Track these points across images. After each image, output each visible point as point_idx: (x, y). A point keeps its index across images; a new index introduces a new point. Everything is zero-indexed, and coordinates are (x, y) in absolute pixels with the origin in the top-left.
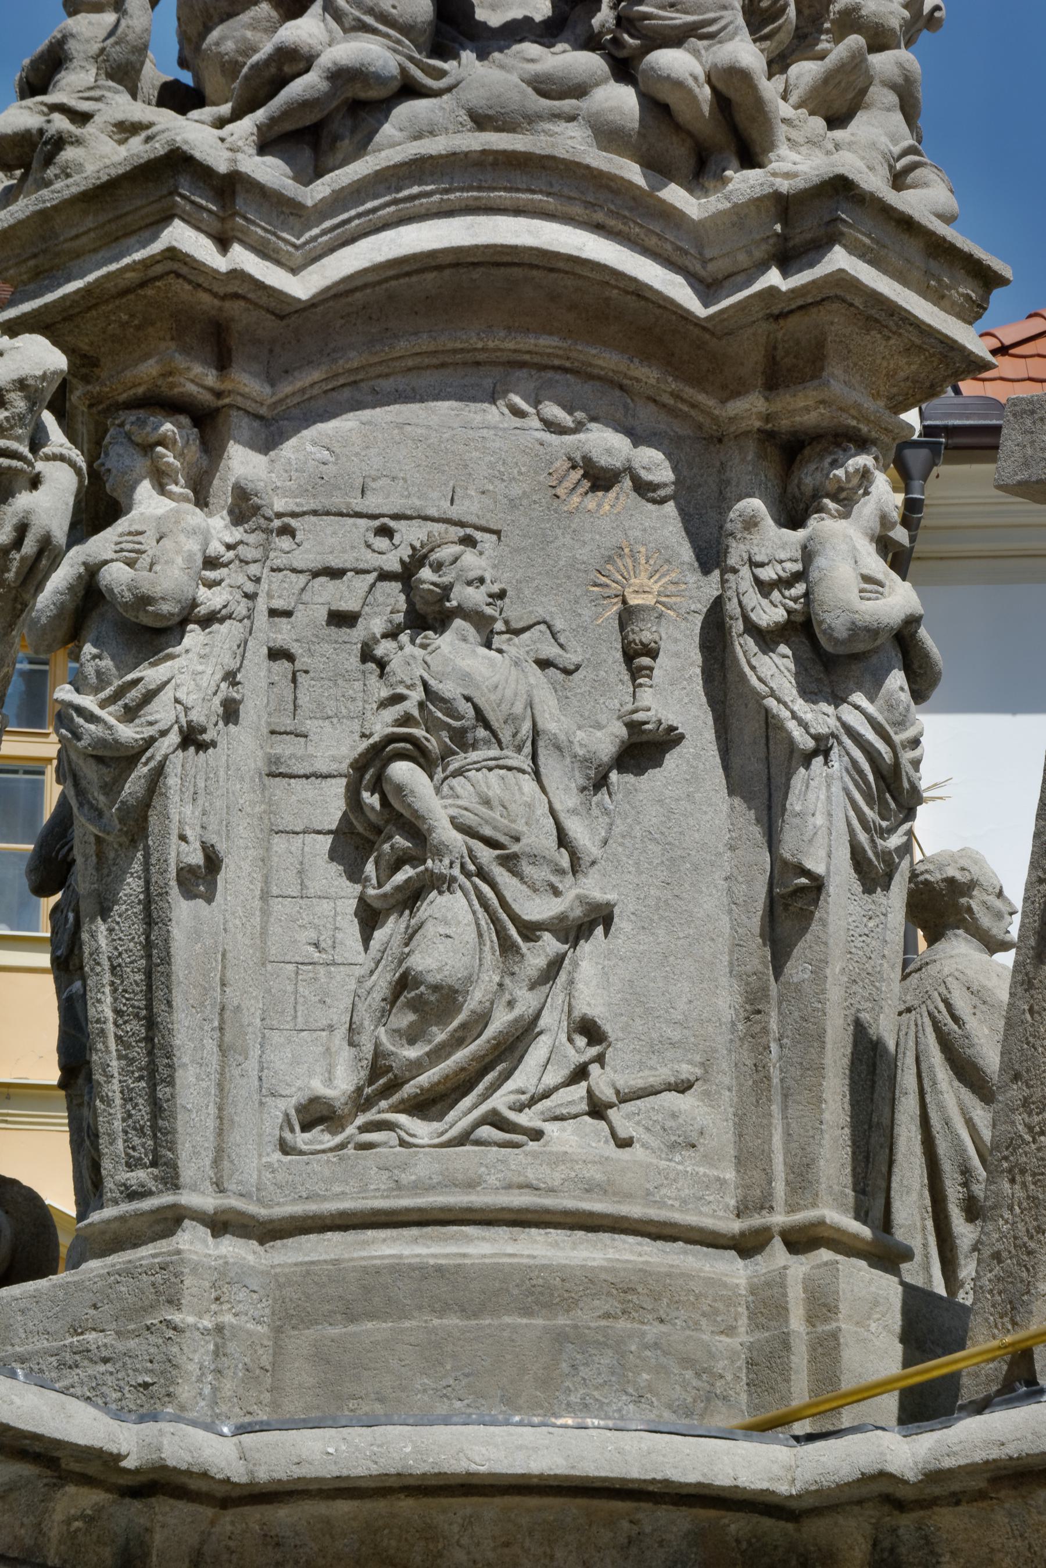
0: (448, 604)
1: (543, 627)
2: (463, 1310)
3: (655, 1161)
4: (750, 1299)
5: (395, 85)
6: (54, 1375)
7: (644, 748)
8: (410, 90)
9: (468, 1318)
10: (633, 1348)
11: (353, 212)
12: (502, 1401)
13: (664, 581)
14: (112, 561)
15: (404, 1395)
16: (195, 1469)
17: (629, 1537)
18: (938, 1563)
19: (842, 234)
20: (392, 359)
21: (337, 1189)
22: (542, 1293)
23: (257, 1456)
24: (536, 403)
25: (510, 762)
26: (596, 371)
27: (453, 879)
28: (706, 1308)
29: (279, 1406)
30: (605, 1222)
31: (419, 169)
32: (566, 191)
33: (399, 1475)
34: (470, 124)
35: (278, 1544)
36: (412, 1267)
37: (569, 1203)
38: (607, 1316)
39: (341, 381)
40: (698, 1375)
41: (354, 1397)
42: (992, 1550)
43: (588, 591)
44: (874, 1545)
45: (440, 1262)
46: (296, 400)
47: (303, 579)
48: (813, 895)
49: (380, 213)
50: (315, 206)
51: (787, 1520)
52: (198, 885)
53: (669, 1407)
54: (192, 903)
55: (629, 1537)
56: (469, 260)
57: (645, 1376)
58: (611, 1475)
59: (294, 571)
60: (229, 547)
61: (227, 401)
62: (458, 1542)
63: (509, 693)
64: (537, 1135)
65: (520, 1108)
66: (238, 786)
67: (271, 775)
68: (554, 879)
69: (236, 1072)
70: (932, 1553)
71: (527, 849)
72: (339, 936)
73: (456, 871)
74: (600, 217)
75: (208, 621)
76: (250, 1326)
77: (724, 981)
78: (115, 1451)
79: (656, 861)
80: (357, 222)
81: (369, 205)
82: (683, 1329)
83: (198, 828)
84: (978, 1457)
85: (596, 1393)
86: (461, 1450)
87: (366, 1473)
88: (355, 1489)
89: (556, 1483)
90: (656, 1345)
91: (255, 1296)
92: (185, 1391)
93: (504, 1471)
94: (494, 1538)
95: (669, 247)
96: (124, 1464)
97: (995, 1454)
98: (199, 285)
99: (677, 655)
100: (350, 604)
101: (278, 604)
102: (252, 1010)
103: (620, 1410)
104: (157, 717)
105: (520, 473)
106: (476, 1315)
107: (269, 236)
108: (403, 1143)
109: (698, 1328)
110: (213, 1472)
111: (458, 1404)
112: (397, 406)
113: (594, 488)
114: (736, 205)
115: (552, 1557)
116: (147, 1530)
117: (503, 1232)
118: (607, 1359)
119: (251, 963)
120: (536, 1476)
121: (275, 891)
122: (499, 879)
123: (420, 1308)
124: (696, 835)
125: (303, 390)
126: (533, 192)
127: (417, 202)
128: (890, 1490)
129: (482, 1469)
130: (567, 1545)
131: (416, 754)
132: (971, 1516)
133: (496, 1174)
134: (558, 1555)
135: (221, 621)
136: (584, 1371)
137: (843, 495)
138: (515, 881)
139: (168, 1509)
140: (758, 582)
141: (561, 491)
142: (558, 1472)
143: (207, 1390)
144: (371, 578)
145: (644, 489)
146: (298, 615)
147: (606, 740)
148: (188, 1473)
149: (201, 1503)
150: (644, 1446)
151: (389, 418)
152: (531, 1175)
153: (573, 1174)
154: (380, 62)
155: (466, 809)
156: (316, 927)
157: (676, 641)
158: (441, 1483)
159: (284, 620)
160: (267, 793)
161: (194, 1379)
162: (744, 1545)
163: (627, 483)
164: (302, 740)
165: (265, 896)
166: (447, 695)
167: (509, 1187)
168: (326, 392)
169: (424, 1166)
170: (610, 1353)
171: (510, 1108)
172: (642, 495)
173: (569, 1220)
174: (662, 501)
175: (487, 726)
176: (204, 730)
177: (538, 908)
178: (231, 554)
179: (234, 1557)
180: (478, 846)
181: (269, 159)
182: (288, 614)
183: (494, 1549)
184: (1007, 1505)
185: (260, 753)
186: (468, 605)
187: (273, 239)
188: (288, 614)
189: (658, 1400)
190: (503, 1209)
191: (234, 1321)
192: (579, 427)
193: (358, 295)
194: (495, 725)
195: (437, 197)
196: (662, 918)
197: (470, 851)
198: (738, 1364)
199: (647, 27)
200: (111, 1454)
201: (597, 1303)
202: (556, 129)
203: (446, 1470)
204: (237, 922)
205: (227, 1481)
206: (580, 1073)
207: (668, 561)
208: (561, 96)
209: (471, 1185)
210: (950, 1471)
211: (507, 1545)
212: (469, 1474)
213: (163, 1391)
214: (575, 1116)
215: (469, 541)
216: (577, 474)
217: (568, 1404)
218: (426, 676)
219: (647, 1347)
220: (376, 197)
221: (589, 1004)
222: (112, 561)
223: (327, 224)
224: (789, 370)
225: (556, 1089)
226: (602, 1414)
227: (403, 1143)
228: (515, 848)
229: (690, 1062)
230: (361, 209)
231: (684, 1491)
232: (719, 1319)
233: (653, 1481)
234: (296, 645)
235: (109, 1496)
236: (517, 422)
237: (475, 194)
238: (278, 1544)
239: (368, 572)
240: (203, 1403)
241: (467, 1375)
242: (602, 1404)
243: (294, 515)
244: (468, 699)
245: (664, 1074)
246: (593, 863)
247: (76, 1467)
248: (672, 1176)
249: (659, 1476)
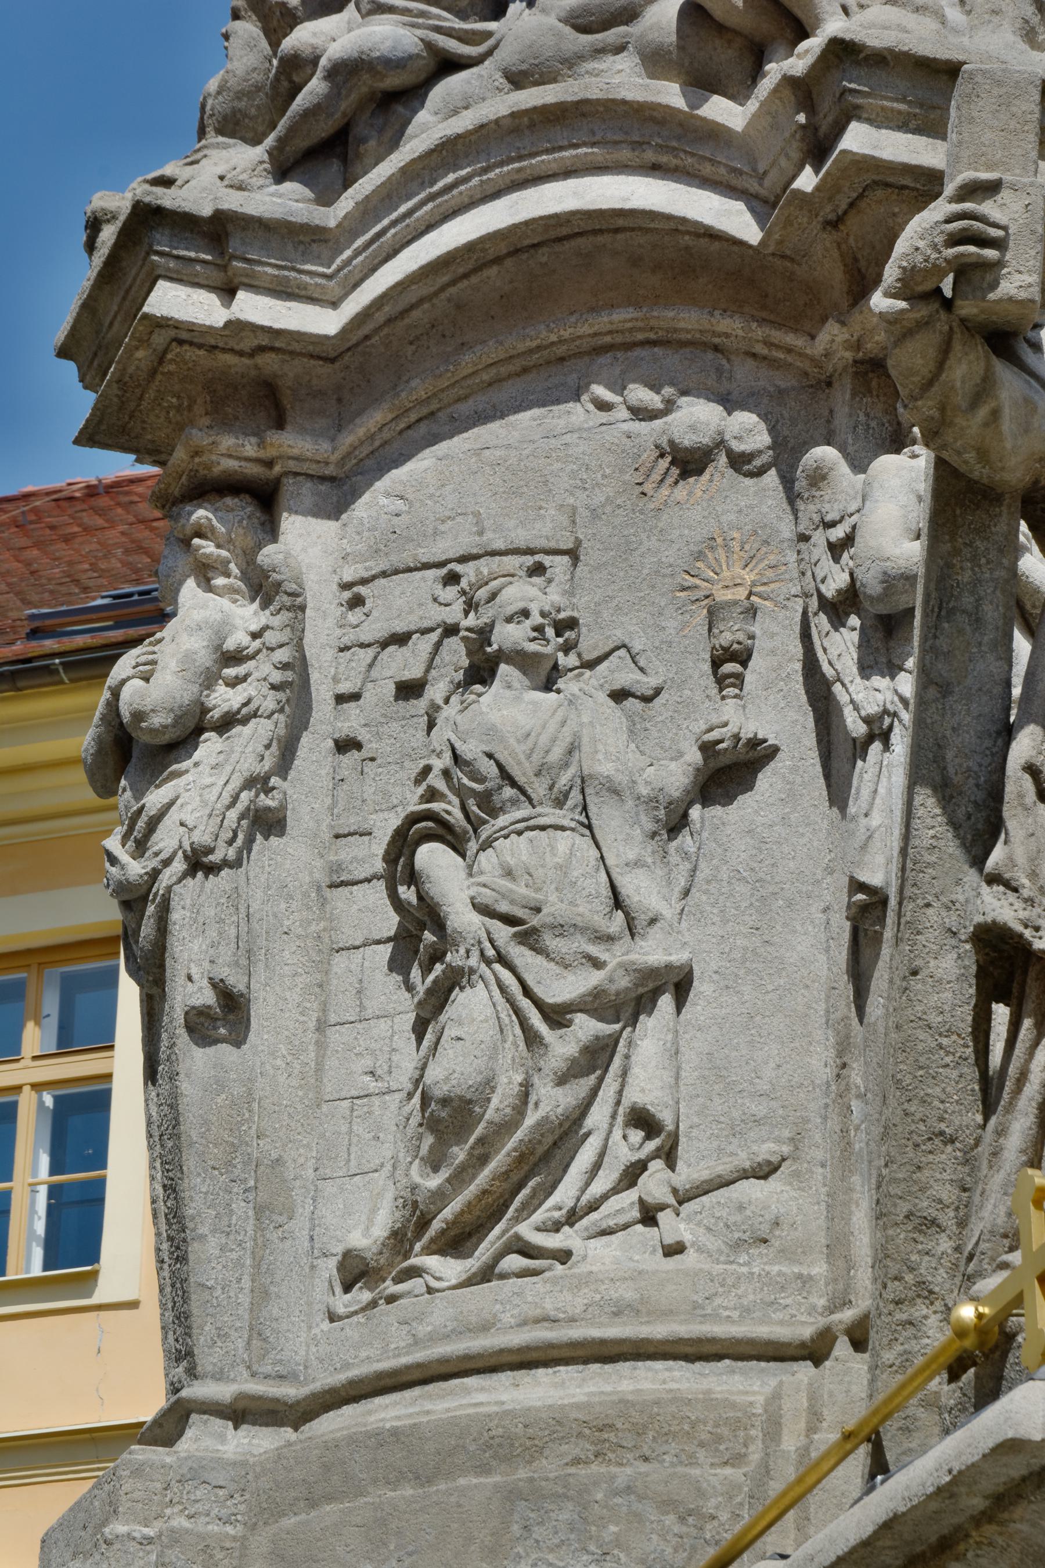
0: (489, 649)
1: (622, 652)
2: (417, 1478)
3: (706, 1267)
5: (427, 64)
7: (729, 772)
8: (448, 65)
9: (422, 1486)
10: (599, 1496)
11: (386, 222)
13: (761, 566)
14: (129, 679)
19: (857, 107)
20: (465, 378)
22: (500, 1445)
24: (620, 390)
25: (541, 821)
26: (683, 336)
27: (472, 971)
28: (704, 1436)
30: (625, 1349)
31: (449, 152)
32: (610, 136)
34: (508, 86)
36: (369, 1435)
37: (576, 1333)
38: (577, 1461)
39: (413, 417)
40: (682, 1519)
43: (675, 598)
45: (395, 1424)
46: (365, 450)
47: (371, 652)
48: (878, 912)
50: (339, 225)
52: (215, 1028)
54: (211, 1050)
56: (527, 242)
57: (613, 1528)
59: (363, 646)
60: (255, 636)
61: (277, 469)
63: (544, 740)
64: (564, 1256)
65: (556, 1227)
66: (283, 906)
67: (333, 886)
68: (594, 950)
69: (274, 1236)
71: (549, 920)
72: (395, 1058)
73: (474, 961)
74: (650, 156)
75: (227, 723)
76: (215, 1528)
77: (819, 1034)
79: (744, 904)
80: (393, 231)
81: (403, 209)
82: (673, 1465)
83: (206, 965)
85: (551, 1557)
90: (629, 1490)
91: (221, 1492)
95: (722, 170)
98: (215, 347)
99: (773, 652)
100: (415, 672)
101: (345, 688)
102: (302, 1160)
104: (161, 845)
105: (604, 476)
106: (429, 1481)
107: (286, 273)
109: (692, 1461)
112: (476, 430)
113: (685, 475)
117: (505, 1378)
118: (566, 1514)
119: (299, 1107)
121: (333, 1018)
122: (518, 962)
123: (375, 1481)
124: (792, 864)
125: (372, 437)
126: (576, 146)
127: (455, 192)
131: (441, 831)
133: (513, 1309)
135: (245, 721)
136: (538, 1532)
138: (540, 960)
141: (648, 487)
144: (434, 636)
145: (739, 462)
146: (366, 695)
147: (676, 775)
151: (467, 446)
152: (549, 1306)
153: (598, 1297)
154: (388, 44)
155: (485, 886)
156: (373, 1053)
157: (773, 635)
159: (353, 704)
160: (328, 908)
163: (723, 459)
164: (366, 838)
165: (322, 1026)
167: (524, 1323)
168: (401, 432)
169: (441, 1313)
170: (570, 1505)
171: (538, 1229)
172: (738, 470)
173: (580, 1353)
174: (760, 473)
175: (514, 784)
176: (210, 851)
177: (563, 987)
178: (257, 644)
180: (496, 925)
181: (289, 186)
182: (355, 697)
185: (319, 863)
186: (507, 645)
187: (293, 274)
188: (355, 697)
189: (628, 1555)
190: (502, 1351)
191: (186, 1524)
192: (670, 406)
193: (416, 314)
194: (521, 780)
195: (476, 181)
196: (749, 971)
198: (739, 1499)
201: (565, 1447)
204: (279, 1062)
206: (633, 1173)
207: (766, 542)
208: (605, 25)
209: (485, 1327)
214: (626, 1227)
215: (538, 570)
216: (664, 463)
218: (454, 739)
219: (617, 1493)
220: (409, 198)
221: (643, 1090)
222: (129, 679)
223: (359, 242)
225: (605, 1197)
227: (430, 1290)
228: (535, 921)
229: (778, 1140)
232: (722, 1447)
234: (363, 731)
236: (604, 417)
237: (516, 165)
239: (431, 630)
241: (410, 1554)
243: (364, 582)
244: (490, 756)
245: (743, 1160)
246: (653, 921)
248: (730, 1281)
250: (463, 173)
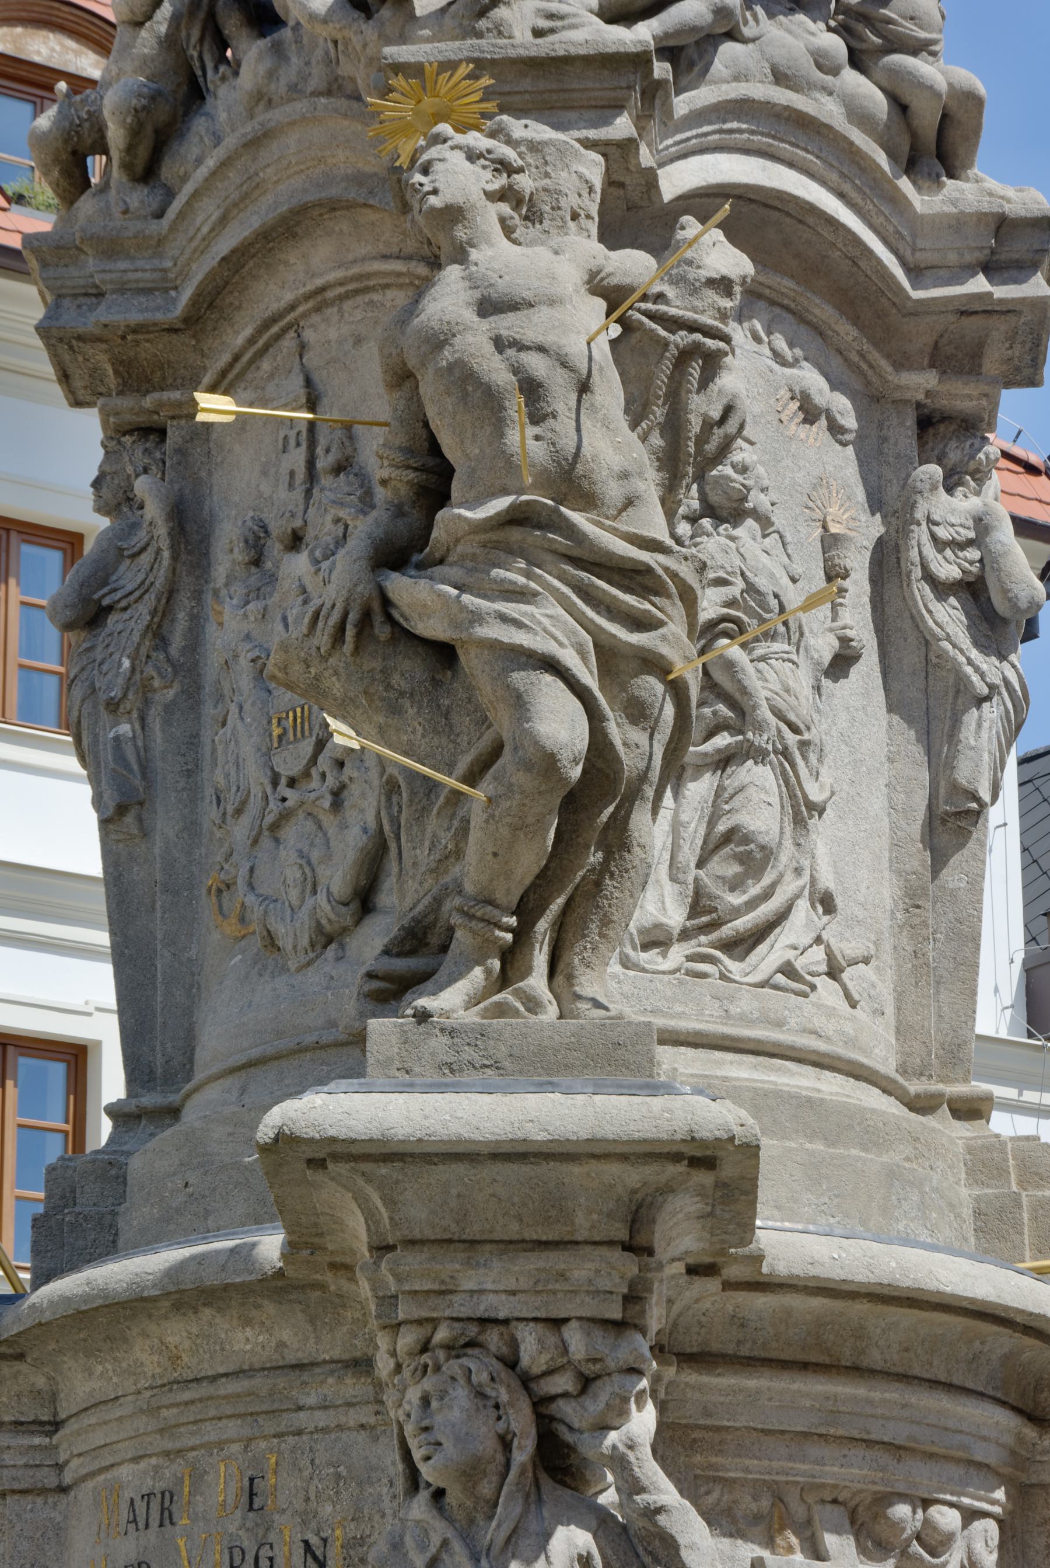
4: (968, 1157)
9: (829, 1146)
11: (694, 132)
21: (678, 1008)
24: (769, 333)
26: (810, 317)
32: (831, 159)
34: (771, 78)
35: (742, 1325)
36: (792, 1096)
48: (974, 818)
49: (710, 138)
74: (847, 188)
77: (886, 874)
87: (866, 1280)
88: (832, 1290)
95: (891, 229)
108: (723, 977)
113: (805, 421)
114: (962, 213)
123: (797, 1132)
129: (948, 1290)
134: (935, 1363)
137: (978, 476)
140: (934, 537)
141: (784, 418)
145: (835, 429)
158: (895, 1293)
166: (762, 589)
169: (746, 1002)
172: (833, 435)
174: (844, 444)
180: (784, 728)
192: (795, 364)
195: (745, 136)
197: (779, 731)
199: (891, 30)
202: (823, 100)
211: (906, 1350)
220: (710, 123)
224: (947, 357)
230: (700, 131)
238: (742, 1325)
241: (836, 1196)
244: (776, 596)
250: (744, 126)
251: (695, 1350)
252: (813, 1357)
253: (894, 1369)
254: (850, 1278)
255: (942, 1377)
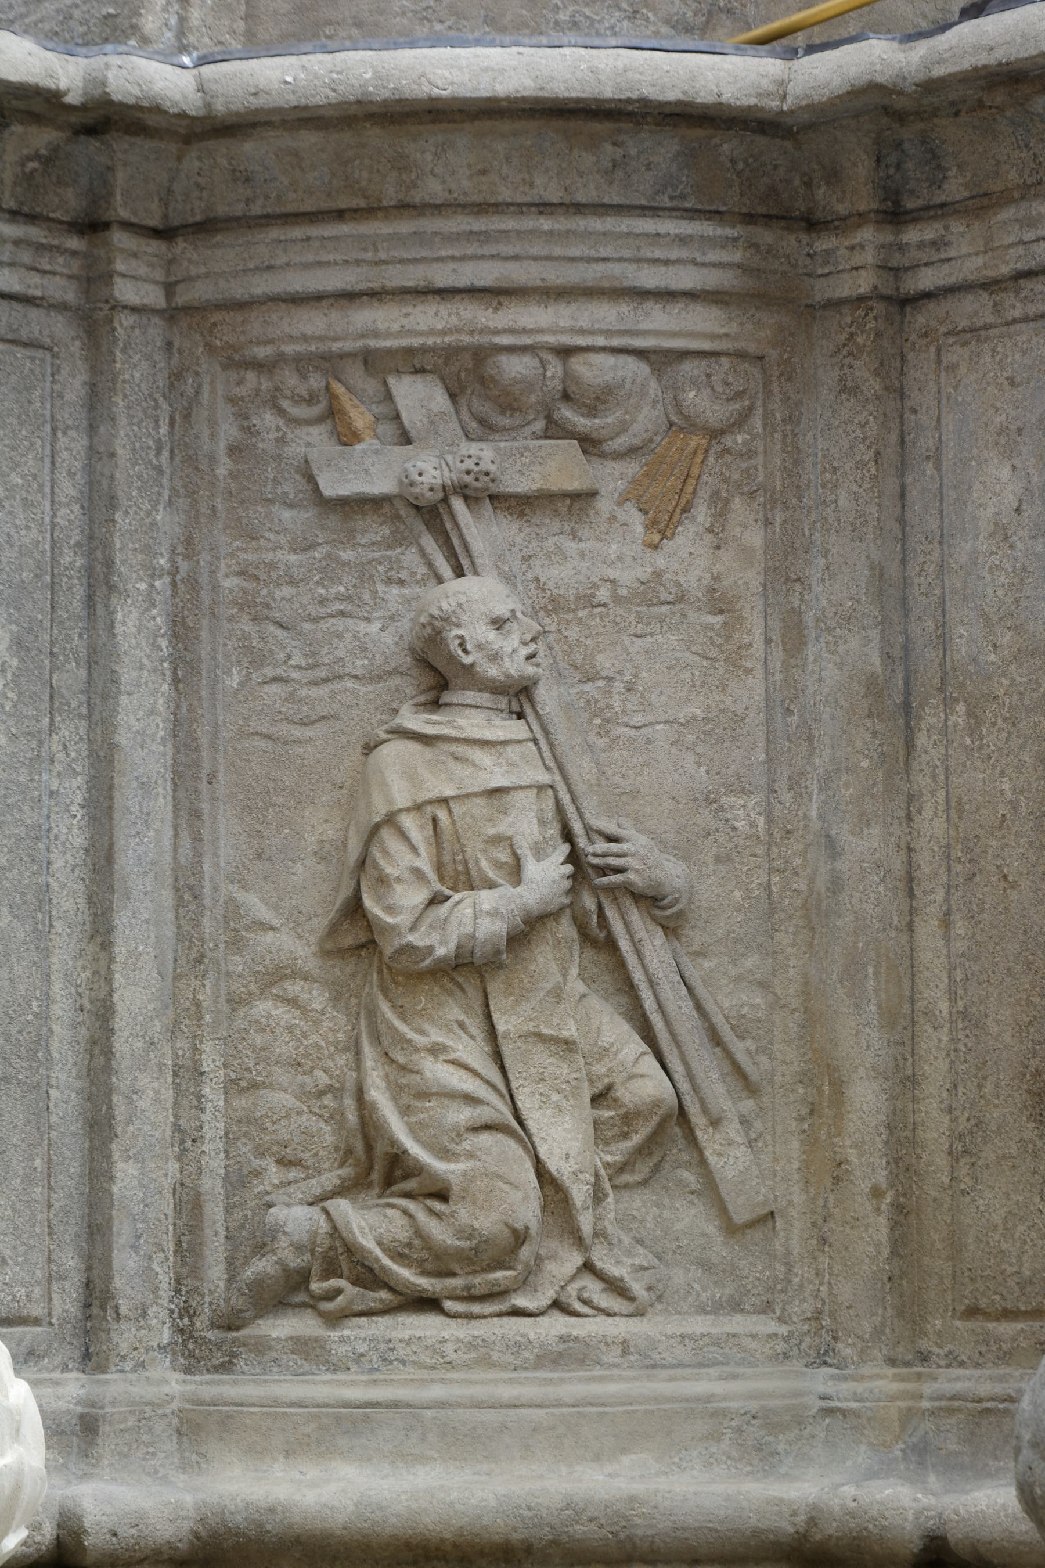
6: (23, 10)
12: (485, 22)
15: (381, 19)
16: (145, 104)
17: (614, 160)
18: (945, 178)
23: (214, 87)
29: (254, 35)
33: (359, 102)
41: (329, 22)
42: (998, 163)
44: (878, 161)
51: (783, 138)
53: (667, 22)
55: (614, 160)
58: (583, 95)
62: (432, 172)
70: (939, 166)
78: (53, 87)
84: (966, 64)
85: (587, 11)
86: (424, 75)
89: (527, 106)
92: (150, 23)
93: (468, 95)
94: (469, 166)
96: (69, 99)
97: (983, 59)
103: (612, 28)
110: (167, 105)
111: (438, 27)
115: (531, 185)
116: (108, 168)
120: (503, 99)
128: (886, 101)
130: (547, 170)
132: (974, 127)
134: (538, 182)
139: (126, 146)
142: (526, 94)
143: (173, 21)
148: (138, 107)
149: (161, 139)
150: (620, 65)
158: (407, 109)
161: (158, 8)
162: (741, 166)
179: (205, 194)
183: (471, 177)
184: (1008, 114)
189: (655, 15)
200: (49, 91)
203: (407, 96)
205: (182, 115)
210: (942, 80)
211: (483, 172)
212: (432, 99)
213: (126, 24)
217: (557, 23)
226: (593, 32)
231: (667, 110)
233: (629, 101)
235: (60, 134)
238: (247, 180)
240: (169, 34)
242: (592, 21)
247: (21, 105)
249: (634, 95)
251: (198, 218)
252: (343, 203)
253: (463, 200)
254: (303, 102)
255: (554, 195)
